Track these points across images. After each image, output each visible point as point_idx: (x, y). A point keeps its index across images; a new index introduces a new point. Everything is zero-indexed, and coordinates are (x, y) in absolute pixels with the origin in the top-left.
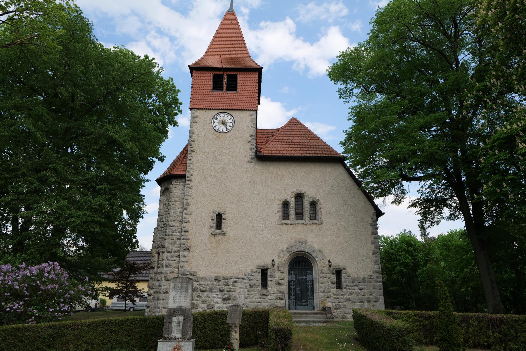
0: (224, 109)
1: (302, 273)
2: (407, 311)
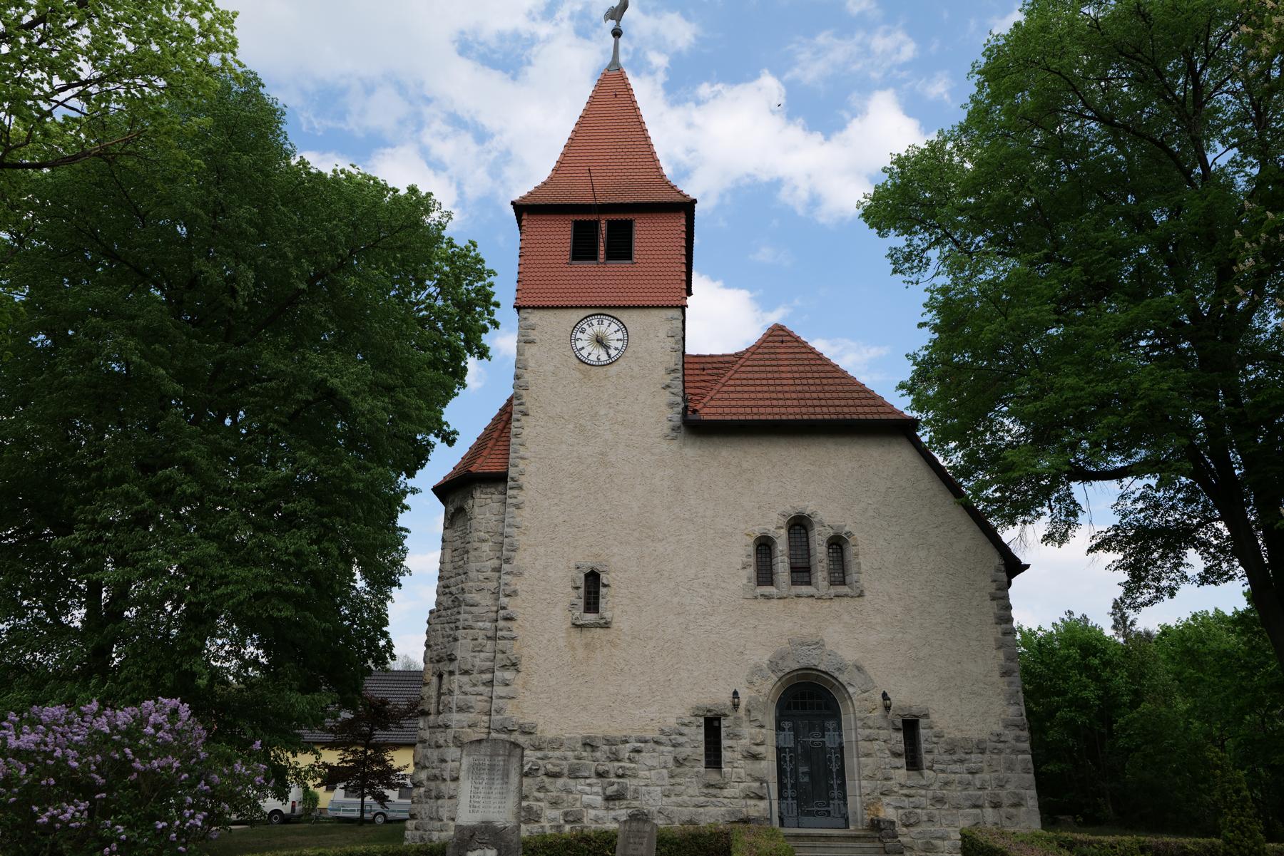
0: (600, 307)
2: (1118, 837)
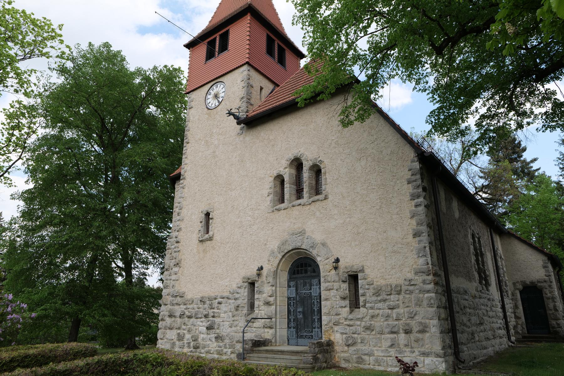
1: (305, 284)
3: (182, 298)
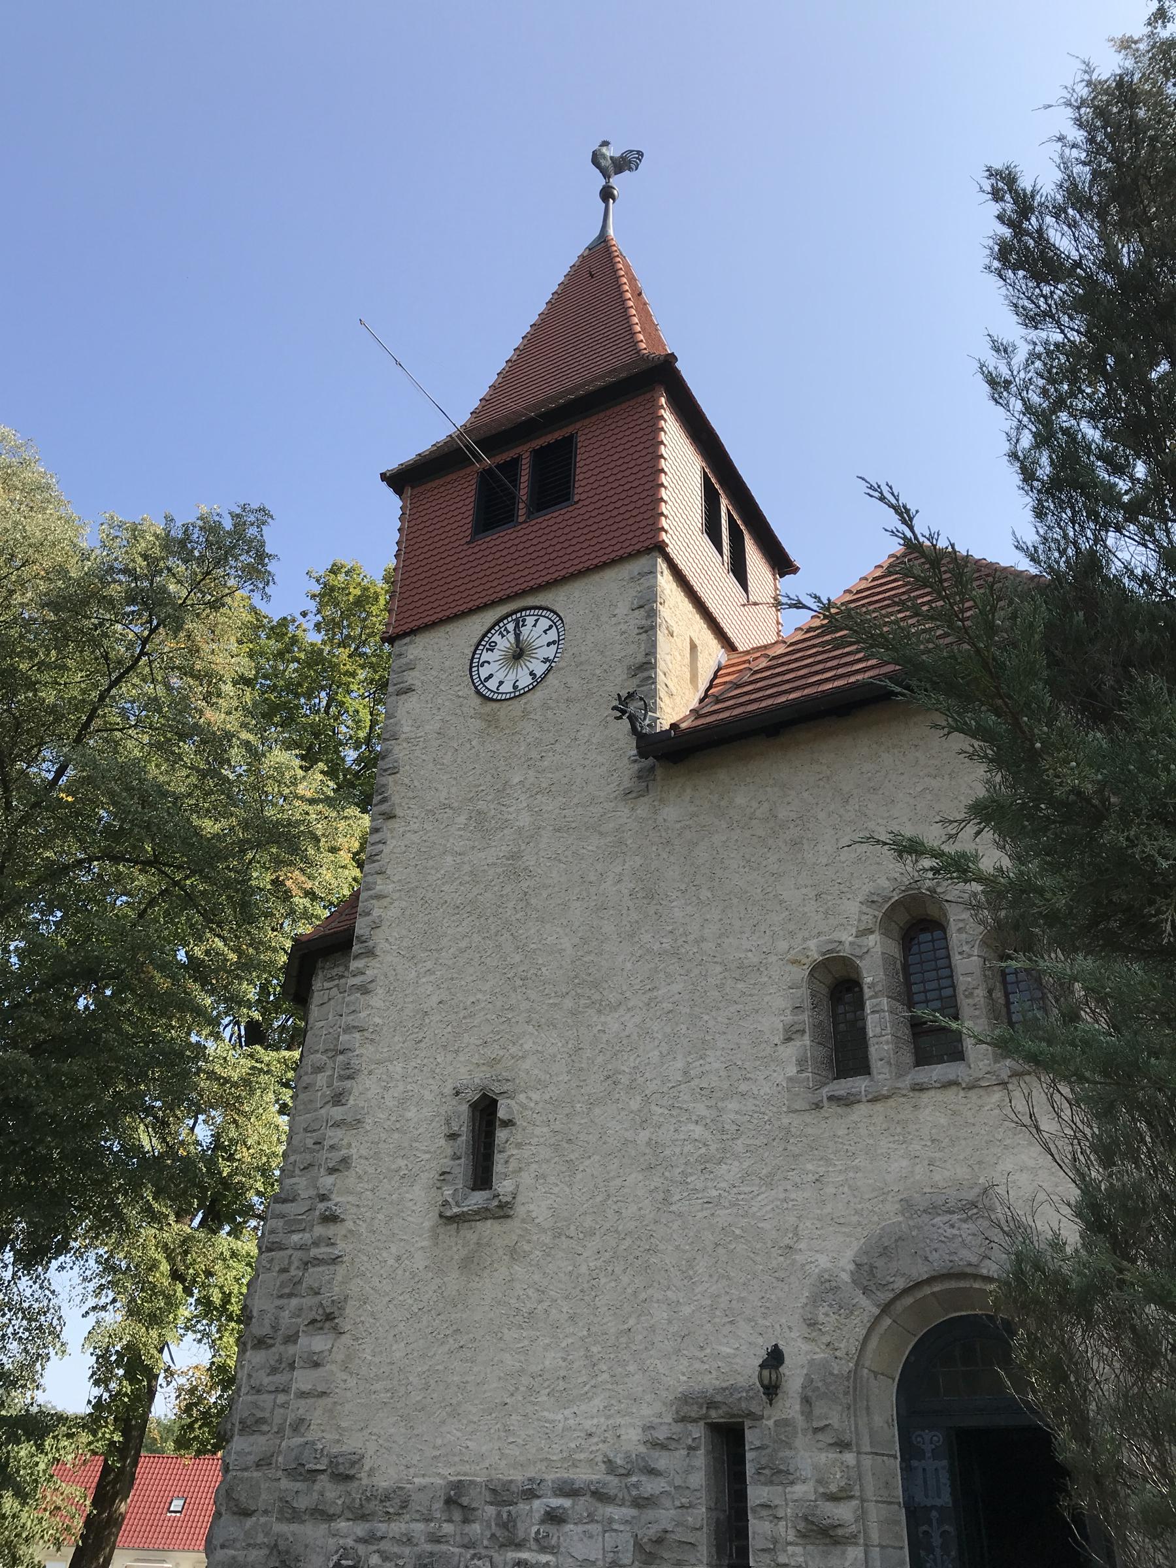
3: (341, 1487)
